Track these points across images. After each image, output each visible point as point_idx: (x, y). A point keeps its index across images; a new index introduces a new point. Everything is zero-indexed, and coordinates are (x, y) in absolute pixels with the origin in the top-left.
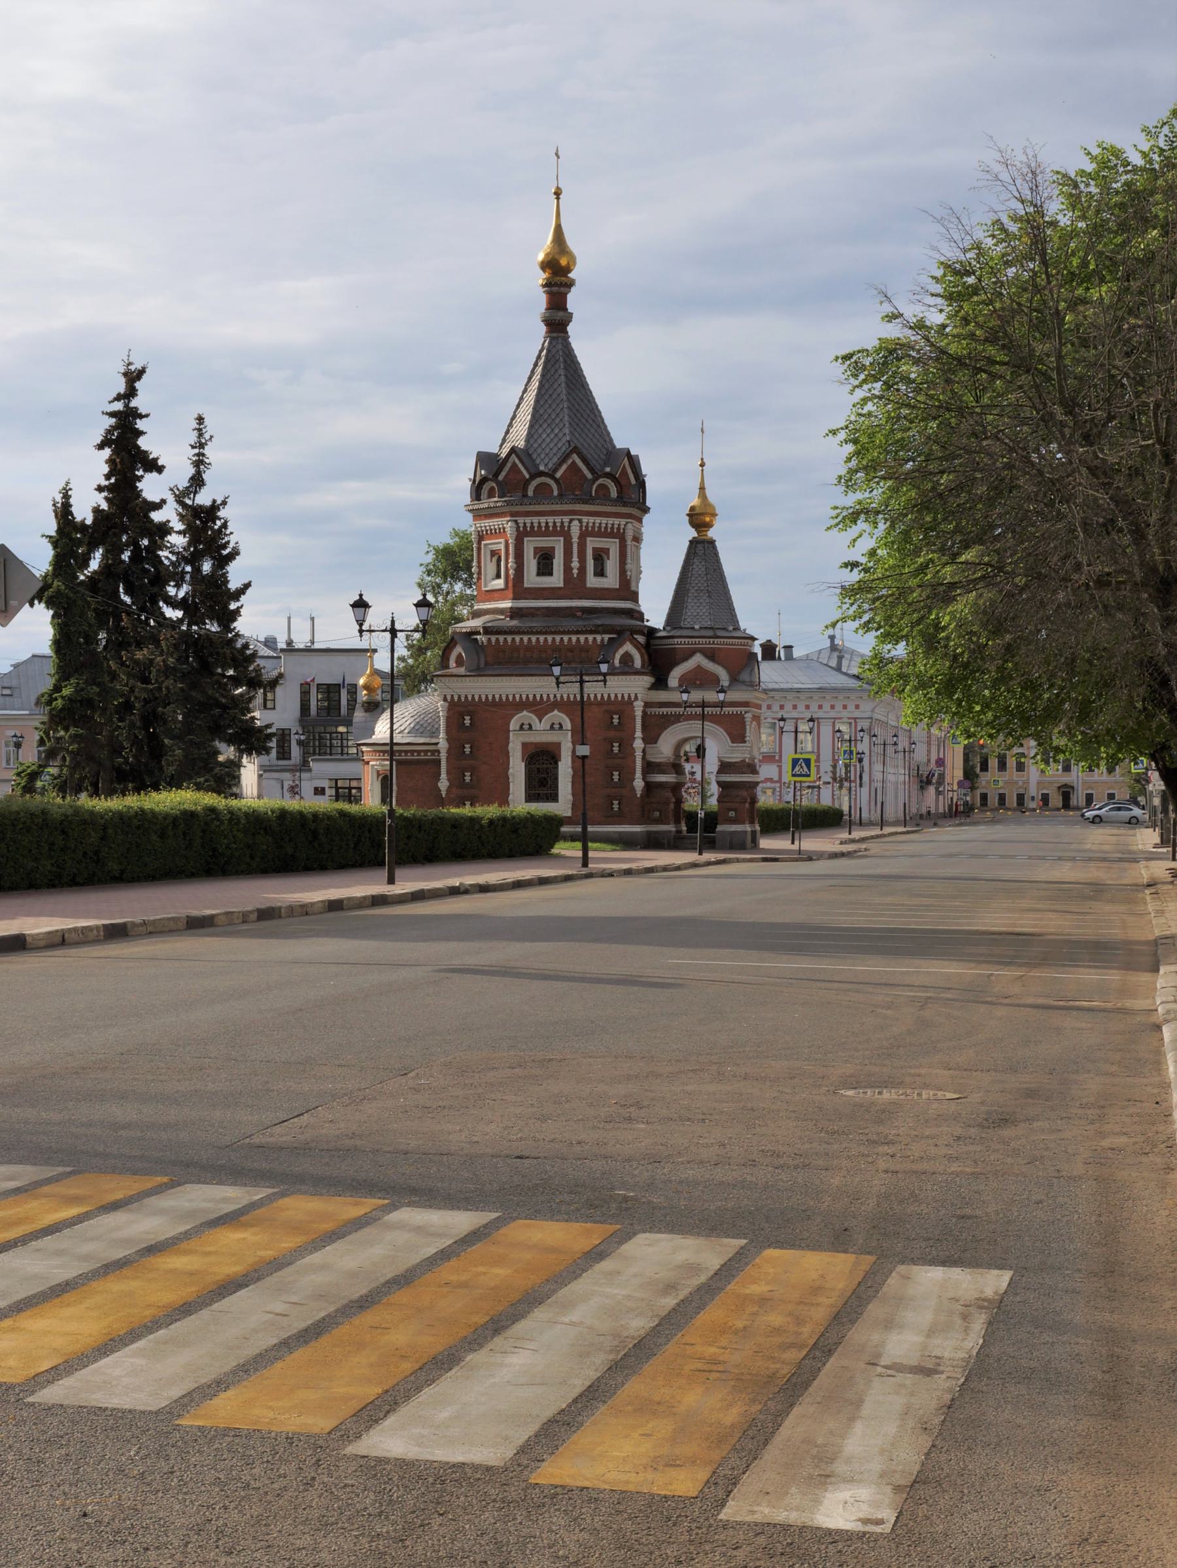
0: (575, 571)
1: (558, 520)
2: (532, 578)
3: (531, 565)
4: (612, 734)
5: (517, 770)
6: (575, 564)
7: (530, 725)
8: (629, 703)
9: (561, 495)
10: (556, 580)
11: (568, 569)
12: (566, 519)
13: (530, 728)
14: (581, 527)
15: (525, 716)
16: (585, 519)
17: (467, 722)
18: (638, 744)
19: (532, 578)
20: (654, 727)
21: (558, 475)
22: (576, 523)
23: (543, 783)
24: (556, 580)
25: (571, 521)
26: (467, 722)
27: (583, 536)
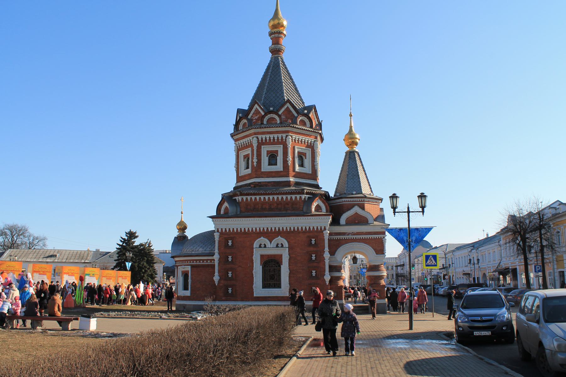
0: (255, 164)
3: (243, 164)
4: (312, 249)
7: (265, 245)
8: (320, 232)
9: (281, 123)
11: (252, 162)
12: (251, 138)
13: (265, 246)
14: (258, 140)
16: (260, 137)
17: (230, 243)
18: (327, 255)
20: (335, 245)
21: (249, 117)
22: (255, 139)
23: (272, 278)
25: (253, 138)
26: (230, 243)
27: (261, 144)
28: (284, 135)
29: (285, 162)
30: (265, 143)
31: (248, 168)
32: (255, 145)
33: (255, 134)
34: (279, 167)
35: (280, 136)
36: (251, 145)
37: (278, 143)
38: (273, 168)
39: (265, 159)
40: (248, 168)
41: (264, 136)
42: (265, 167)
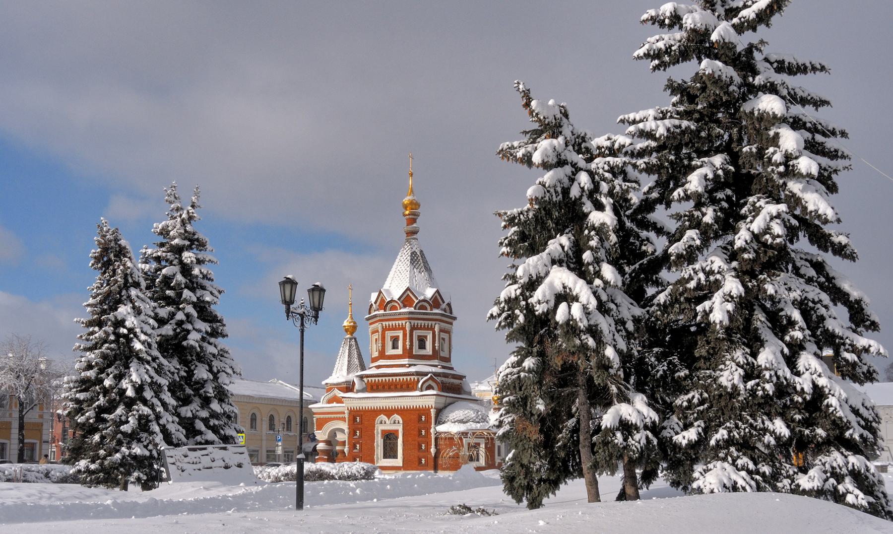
1: (400, 322)
2: (390, 352)
3: (389, 344)
5: (379, 442)
6: (408, 343)
10: (399, 351)
12: (404, 322)
15: (383, 417)
16: (413, 321)
19: (390, 352)
24: (399, 351)
28: (434, 323)
29: (434, 347)
30: (417, 329)
31: (395, 347)
32: (408, 329)
33: (409, 319)
34: (429, 350)
35: (430, 323)
36: (403, 329)
37: (428, 329)
38: (422, 352)
39: (416, 343)
40: (394, 348)
41: (416, 322)
42: (416, 351)
